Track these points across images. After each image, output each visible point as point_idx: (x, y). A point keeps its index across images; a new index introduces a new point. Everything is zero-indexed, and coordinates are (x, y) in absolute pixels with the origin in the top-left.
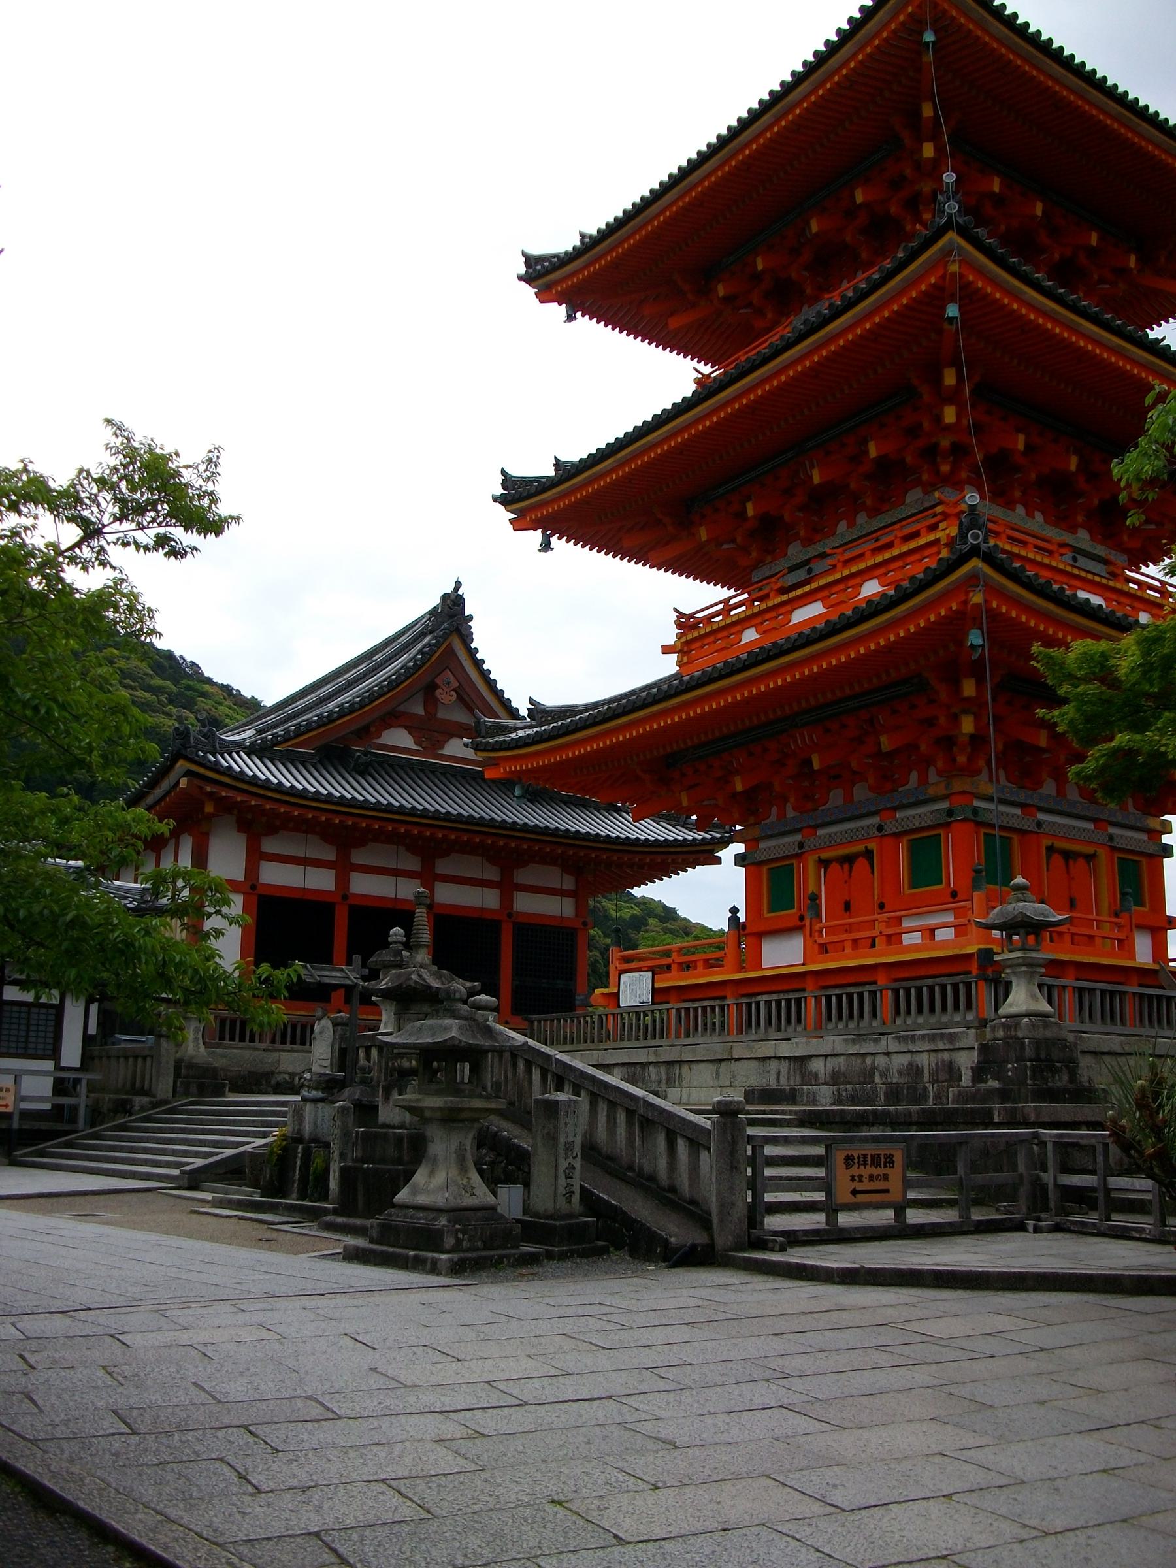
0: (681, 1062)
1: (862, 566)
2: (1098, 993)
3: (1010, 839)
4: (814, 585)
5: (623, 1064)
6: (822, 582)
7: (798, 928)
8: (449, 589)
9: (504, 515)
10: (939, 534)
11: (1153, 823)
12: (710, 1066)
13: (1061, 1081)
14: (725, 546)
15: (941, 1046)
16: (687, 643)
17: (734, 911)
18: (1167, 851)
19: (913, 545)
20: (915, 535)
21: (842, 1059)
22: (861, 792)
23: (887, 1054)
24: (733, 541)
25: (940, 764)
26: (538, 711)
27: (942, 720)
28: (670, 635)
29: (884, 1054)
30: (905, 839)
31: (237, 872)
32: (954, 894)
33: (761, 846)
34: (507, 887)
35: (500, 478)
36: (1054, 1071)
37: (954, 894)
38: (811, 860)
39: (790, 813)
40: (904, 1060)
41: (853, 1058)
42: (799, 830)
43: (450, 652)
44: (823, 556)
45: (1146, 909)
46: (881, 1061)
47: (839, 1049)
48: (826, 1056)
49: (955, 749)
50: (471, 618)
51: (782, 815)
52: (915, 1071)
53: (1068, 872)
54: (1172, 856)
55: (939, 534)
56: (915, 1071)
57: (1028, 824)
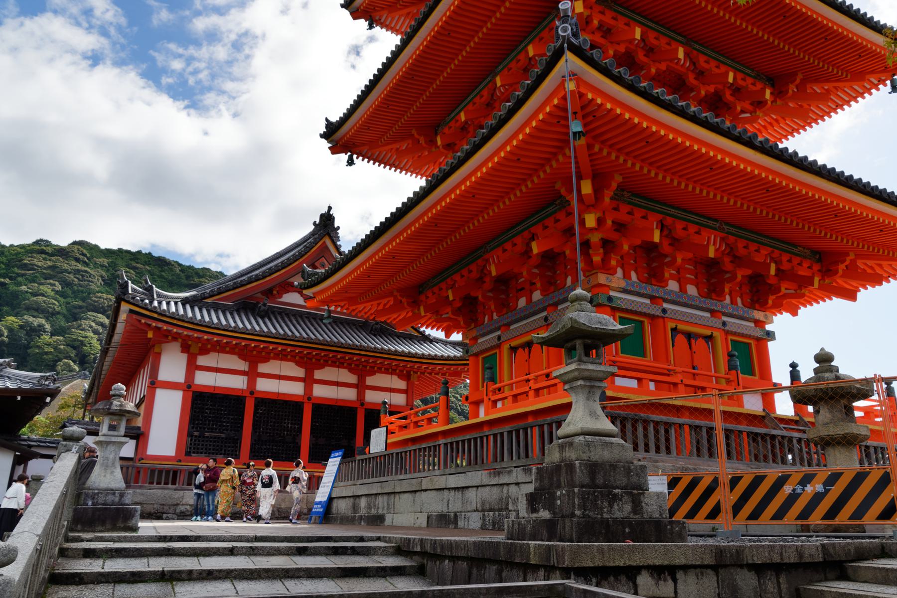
0: (394, 493)
2: (704, 430)
3: (642, 322)
5: (366, 495)
8: (325, 210)
9: (325, 144)
13: (622, 510)
18: (771, 335)
22: (537, 296)
23: (517, 484)
31: (179, 376)
35: (324, 123)
36: (615, 498)
38: (506, 347)
39: (495, 317)
41: (494, 488)
42: (498, 329)
43: (325, 248)
45: (757, 377)
47: (486, 481)
48: (477, 487)
50: (338, 228)
51: (491, 318)
53: (690, 348)
54: (774, 338)
57: (655, 310)
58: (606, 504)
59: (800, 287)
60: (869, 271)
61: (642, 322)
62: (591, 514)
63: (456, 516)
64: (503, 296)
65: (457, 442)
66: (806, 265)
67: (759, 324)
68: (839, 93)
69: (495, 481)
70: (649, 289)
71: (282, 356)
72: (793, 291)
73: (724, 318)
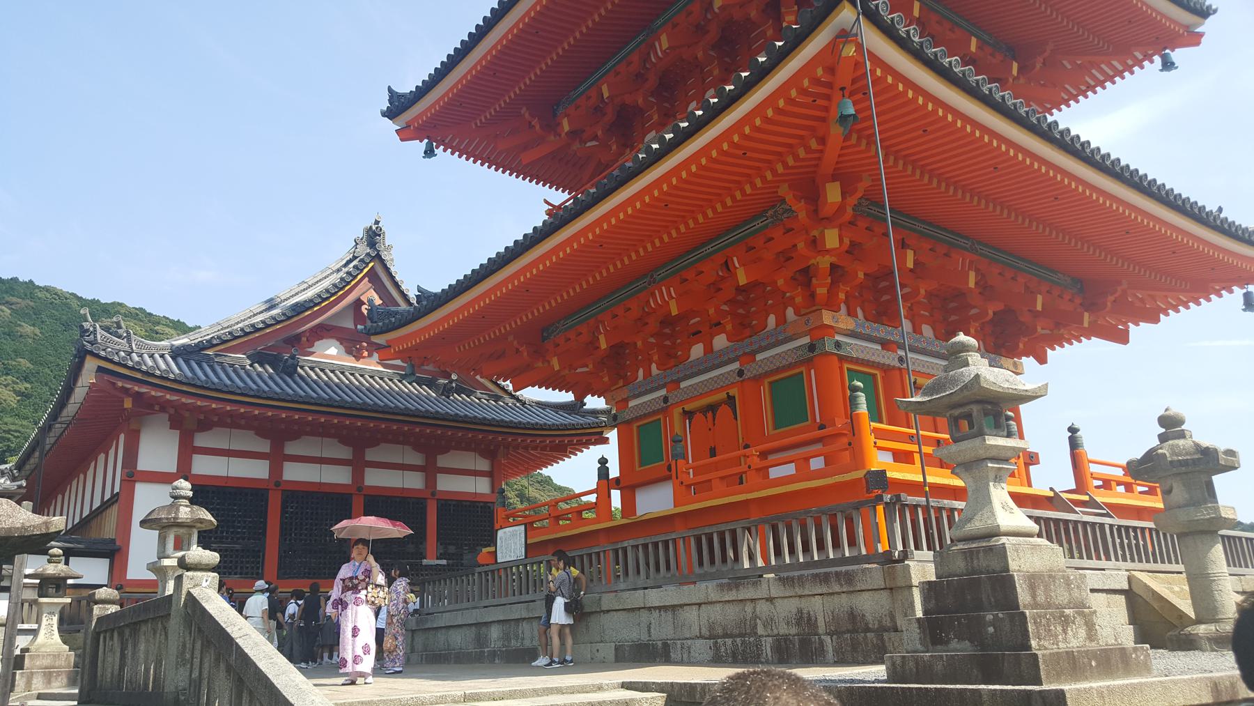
7: (668, 478)
14: (589, 144)
15: (837, 588)
17: (603, 461)
21: (718, 607)
22: (720, 342)
23: (770, 600)
25: (798, 300)
26: (423, 295)
29: (767, 599)
30: (766, 381)
33: (632, 404)
34: (430, 471)
36: (1066, 622)
47: (714, 596)
48: (700, 605)
49: (814, 281)
51: (648, 373)
52: (804, 620)
56: (804, 620)
57: (890, 359)
58: (1059, 629)
60: (1138, 304)
61: (874, 376)
62: (1046, 644)
63: (666, 645)
64: (668, 343)
65: (656, 545)
68: (1094, 71)
70: (882, 331)
71: (320, 431)
72: (1047, 332)
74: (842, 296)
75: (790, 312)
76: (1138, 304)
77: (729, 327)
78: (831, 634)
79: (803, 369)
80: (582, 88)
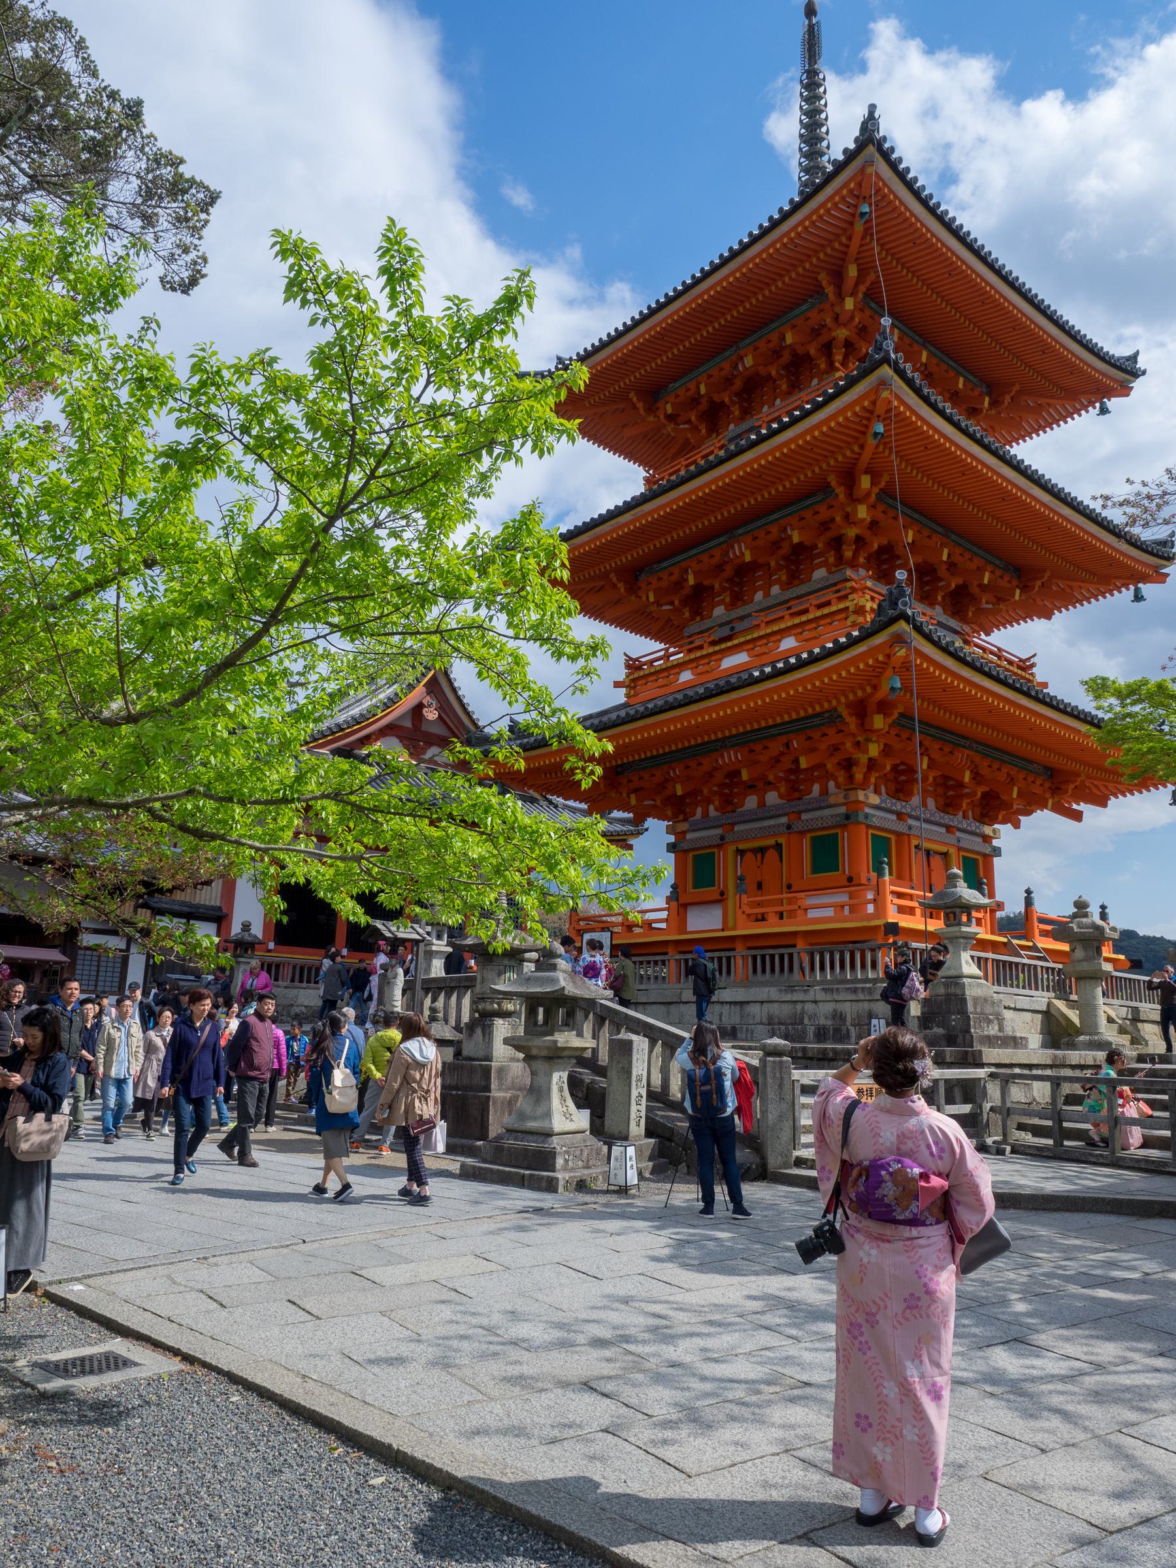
1: (783, 626)
4: (736, 642)
6: (742, 640)
10: (848, 604)
11: (987, 830)
12: (662, 1007)
15: (861, 997)
16: (633, 680)
18: (997, 852)
19: (826, 611)
20: (828, 604)
21: (776, 1005)
22: (772, 798)
23: (815, 1002)
24: (672, 603)
25: (841, 779)
27: (848, 745)
28: (621, 674)
30: (809, 836)
32: (850, 879)
36: (989, 1022)
37: (850, 879)
38: (731, 849)
40: (830, 1007)
44: (742, 618)
46: (809, 1007)
51: (705, 814)
52: (838, 1016)
55: (848, 604)
56: (838, 1016)
57: (901, 827)
59: (1029, 804)
60: (1095, 790)
66: (1038, 782)
67: (987, 839)
69: (788, 997)
70: (898, 806)
73: (958, 834)
74: (873, 780)
75: (831, 784)
76: (1095, 790)
77: (783, 790)
78: (854, 1025)
79: (838, 831)
80: (665, 564)
